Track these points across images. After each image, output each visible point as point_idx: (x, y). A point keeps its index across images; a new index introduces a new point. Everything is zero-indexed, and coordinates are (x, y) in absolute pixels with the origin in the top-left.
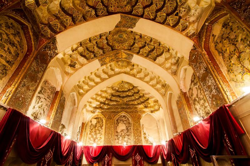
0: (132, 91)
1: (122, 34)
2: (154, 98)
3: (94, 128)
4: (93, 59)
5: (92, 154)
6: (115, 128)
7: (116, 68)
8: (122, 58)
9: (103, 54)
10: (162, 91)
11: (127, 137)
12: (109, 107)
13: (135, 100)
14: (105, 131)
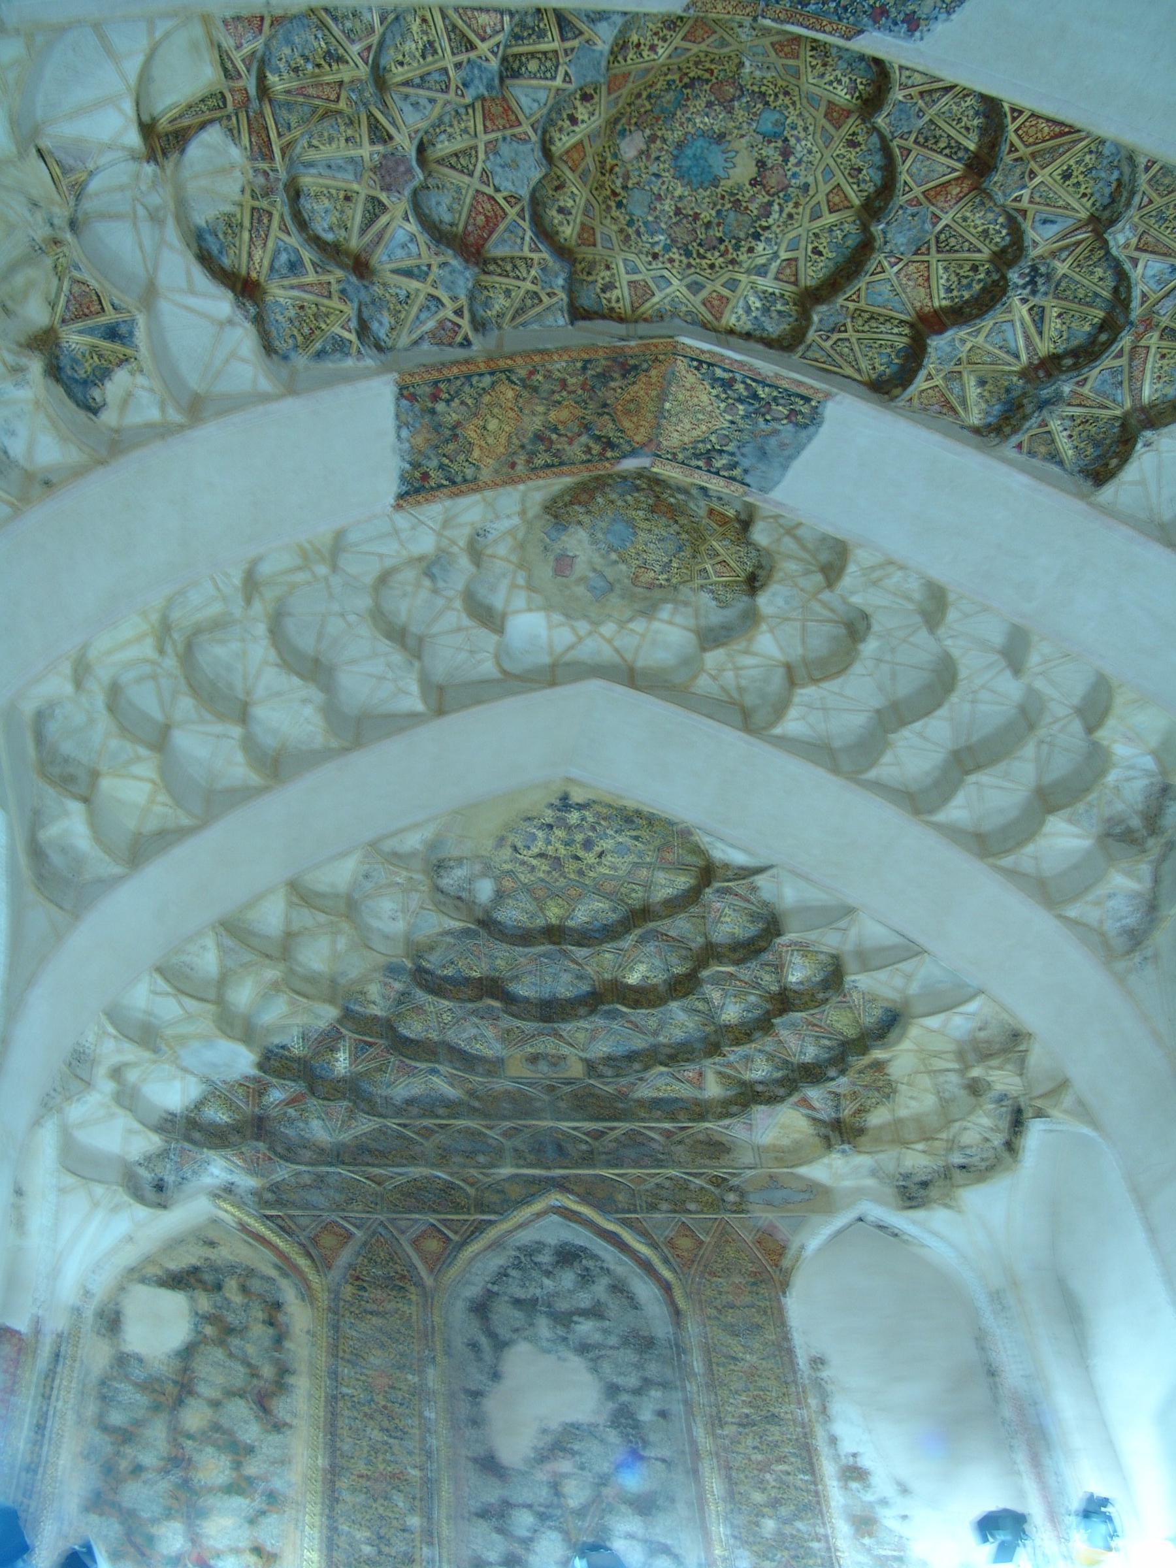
0: (680, 925)
1: (721, 137)
2: (972, 1007)
3: (156, 1408)
4: (329, 365)
6: (464, 1408)
7: (520, 600)
8: (652, 446)
9: (465, 322)
10: (1101, 891)
12: (365, 1125)
13: (713, 1048)
14: (333, 1449)
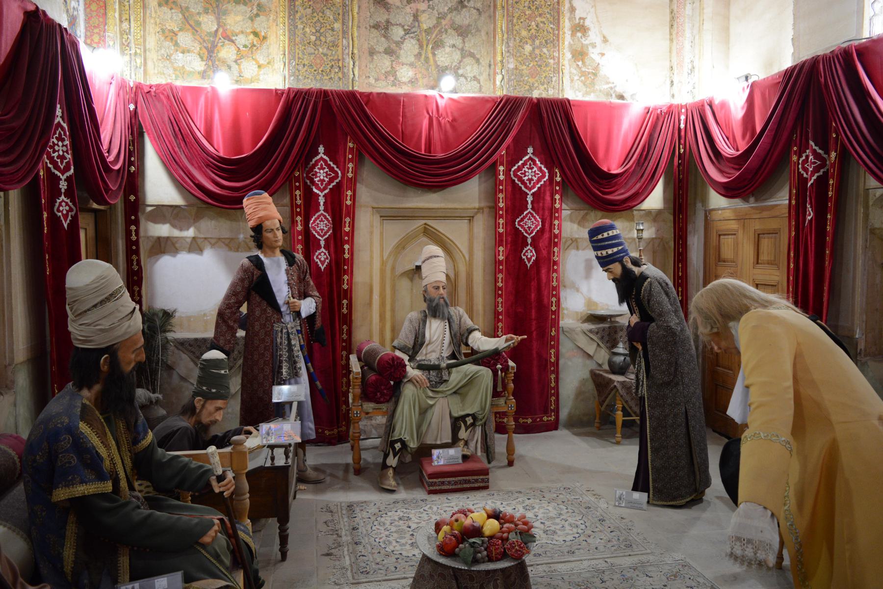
5: (209, 137)
11: (458, 41)
